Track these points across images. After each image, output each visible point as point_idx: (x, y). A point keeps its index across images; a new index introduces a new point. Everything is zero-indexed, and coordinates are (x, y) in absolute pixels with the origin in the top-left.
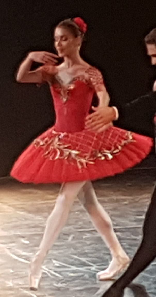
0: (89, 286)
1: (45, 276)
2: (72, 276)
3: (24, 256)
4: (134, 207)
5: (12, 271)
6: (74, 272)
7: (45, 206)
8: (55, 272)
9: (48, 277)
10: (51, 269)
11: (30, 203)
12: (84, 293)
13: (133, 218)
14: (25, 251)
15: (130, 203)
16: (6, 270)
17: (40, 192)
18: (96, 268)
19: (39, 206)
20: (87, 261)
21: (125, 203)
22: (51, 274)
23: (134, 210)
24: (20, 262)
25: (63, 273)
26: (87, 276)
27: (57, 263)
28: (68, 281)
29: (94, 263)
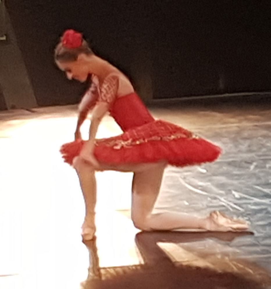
1: (223, 208)
2: (253, 210)
3: (201, 186)
5: (187, 203)
6: (256, 204)
7: (224, 130)
8: (235, 204)
9: (227, 210)
10: (230, 201)
11: (208, 127)
14: (201, 181)
16: (180, 202)
17: (218, 115)
19: (218, 131)
22: (231, 207)
24: (196, 193)
25: (244, 206)
27: (237, 195)
28: (249, 214)
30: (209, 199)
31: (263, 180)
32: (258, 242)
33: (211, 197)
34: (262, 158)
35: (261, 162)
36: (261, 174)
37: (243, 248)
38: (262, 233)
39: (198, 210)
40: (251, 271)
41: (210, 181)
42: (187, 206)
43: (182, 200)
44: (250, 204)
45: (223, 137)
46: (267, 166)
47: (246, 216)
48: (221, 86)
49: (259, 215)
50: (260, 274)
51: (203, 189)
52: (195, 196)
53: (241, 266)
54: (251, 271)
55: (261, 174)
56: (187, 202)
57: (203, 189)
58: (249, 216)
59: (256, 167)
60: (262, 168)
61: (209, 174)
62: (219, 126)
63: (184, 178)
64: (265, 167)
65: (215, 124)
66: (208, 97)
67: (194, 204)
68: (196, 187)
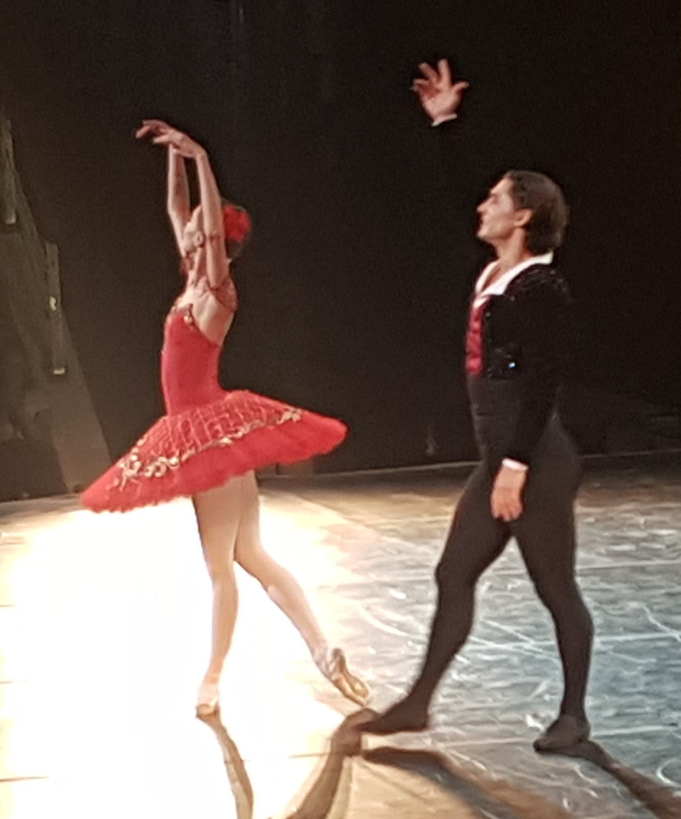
0: (520, 680)
2: (487, 662)
4: (607, 529)
6: (491, 652)
7: (435, 525)
11: (407, 521)
12: (510, 693)
13: (602, 550)
15: (597, 521)
17: (426, 501)
18: (535, 646)
20: (517, 631)
21: (591, 520)
23: (607, 534)
24: (388, 634)
26: (515, 660)
29: (529, 635)
30: (410, 643)
31: (502, 612)
32: (495, 717)
33: (414, 641)
34: (502, 573)
35: (498, 579)
36: (499, 601)
37: (470, 727)
38: (501, 701)
39: (391, 663)
40: (482, 767)
41: (412, 612)
42: (372, 656)
43: (364, 645)
44: (479, 651)
45: (434, 537)
46: (510, 586)
47: (473, 673)
48: (430, 450)
49: (496, 671)
50: (497, 772)
51: (401, 626)
52: (385, 638)
53: (466, 758)
54: (482, 767)
55: (499, 601)
56: (373, 647)
57: (401, 626)
58: (479, 674)
59: (491, 588)
60: (499, 590)
61: (409, 601)
62: (426, 518)
63: (368, 609)
64: (505, 589)
65: (419, 516)
66: (405, 469)
67: (383, 652)
68: (389, 623)
